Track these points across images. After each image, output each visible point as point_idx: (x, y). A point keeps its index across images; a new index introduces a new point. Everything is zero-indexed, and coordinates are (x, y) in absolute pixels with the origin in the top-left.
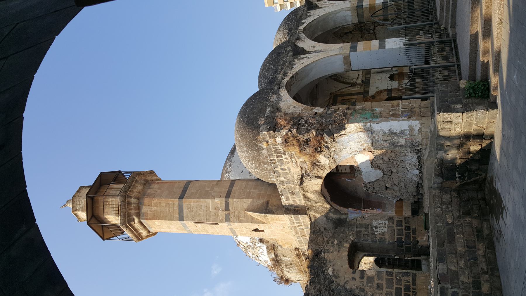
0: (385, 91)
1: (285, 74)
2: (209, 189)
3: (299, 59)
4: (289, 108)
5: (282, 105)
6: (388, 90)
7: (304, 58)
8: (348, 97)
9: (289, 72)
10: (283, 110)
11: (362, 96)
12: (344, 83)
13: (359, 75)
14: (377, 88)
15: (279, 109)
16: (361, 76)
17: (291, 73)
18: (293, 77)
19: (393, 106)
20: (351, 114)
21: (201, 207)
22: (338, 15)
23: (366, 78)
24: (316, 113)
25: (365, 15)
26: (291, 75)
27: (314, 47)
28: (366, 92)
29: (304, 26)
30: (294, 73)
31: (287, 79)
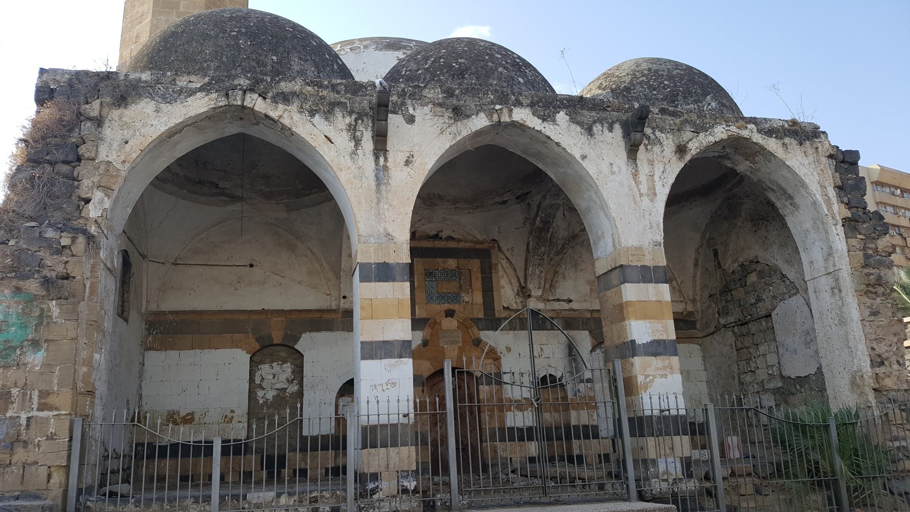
0: (499, 367)
1: (285, 98)
2: (181, 9)
3: (352, 129)
4: (124, 126)
6: (499, 375)
7: (357, 142)
8: (477, 284)
9: (294, 107)
10: (115, 113)
12: (526, 269)
13: (570, 301)
14: (509, 349)
16: (566, 306)
17: (291, 117)
18: (272, 119)
20: (18, 290)
21: (143, 4)
22: (602, 214)
24: (87, 201)
25: (608, 293)
26: (273, 114)
27: (407, 163)
28: (493, 323)
29: (534, 123)
30: (286, 121)
31: (260, 105)
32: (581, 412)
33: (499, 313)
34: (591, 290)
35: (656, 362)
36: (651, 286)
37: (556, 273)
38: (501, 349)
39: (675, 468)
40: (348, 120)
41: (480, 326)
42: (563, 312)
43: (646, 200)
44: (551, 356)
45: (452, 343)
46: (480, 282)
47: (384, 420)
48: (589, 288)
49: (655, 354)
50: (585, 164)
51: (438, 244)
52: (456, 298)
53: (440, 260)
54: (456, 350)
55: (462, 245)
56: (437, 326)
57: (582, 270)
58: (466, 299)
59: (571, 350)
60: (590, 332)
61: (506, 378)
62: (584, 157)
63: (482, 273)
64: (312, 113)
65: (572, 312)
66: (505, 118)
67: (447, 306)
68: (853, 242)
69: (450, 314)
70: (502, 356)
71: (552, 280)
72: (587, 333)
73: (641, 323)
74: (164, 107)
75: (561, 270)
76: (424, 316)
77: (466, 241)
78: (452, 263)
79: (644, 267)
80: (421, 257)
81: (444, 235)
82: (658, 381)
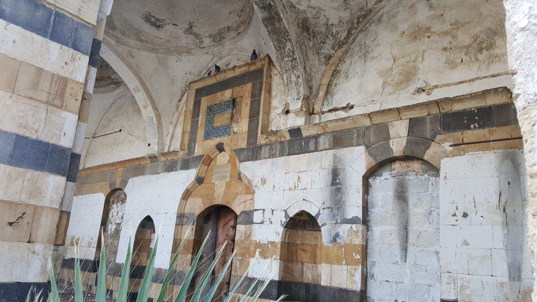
8: (245, 110)
11: (244, 145)
14: (264, 181)
23: (316, 137)
28: (253, 152)
32: (336, 267)
33: (261, 140)
34: (385, 83)
37: (335, 73)
38: (256, 181)
41: (242, 157)
42: (329, 125)
44: (309, 187)
45: (222, 178)
46: (249, 108)
48: (381, 81)
51: (221, 77)
52: (226, 130)
53: (219, 94)
54: (224, 186)
55: (238, 72)
56: (213, 163)
57: (373, 58)
58: (235, 130)
59: (336, 177)
60: (367, 147)
61: (257, 217)
63: (252, 97)
65: (341, 123)
67: (217, 140)
69: (220, 148)
70: (256, 189)
71: (329, 85)
75: (343, 67)
76: (200, 153)
77: (240, 67)
78: (228, 94)
80: (207, 95)
81: (231, 66)
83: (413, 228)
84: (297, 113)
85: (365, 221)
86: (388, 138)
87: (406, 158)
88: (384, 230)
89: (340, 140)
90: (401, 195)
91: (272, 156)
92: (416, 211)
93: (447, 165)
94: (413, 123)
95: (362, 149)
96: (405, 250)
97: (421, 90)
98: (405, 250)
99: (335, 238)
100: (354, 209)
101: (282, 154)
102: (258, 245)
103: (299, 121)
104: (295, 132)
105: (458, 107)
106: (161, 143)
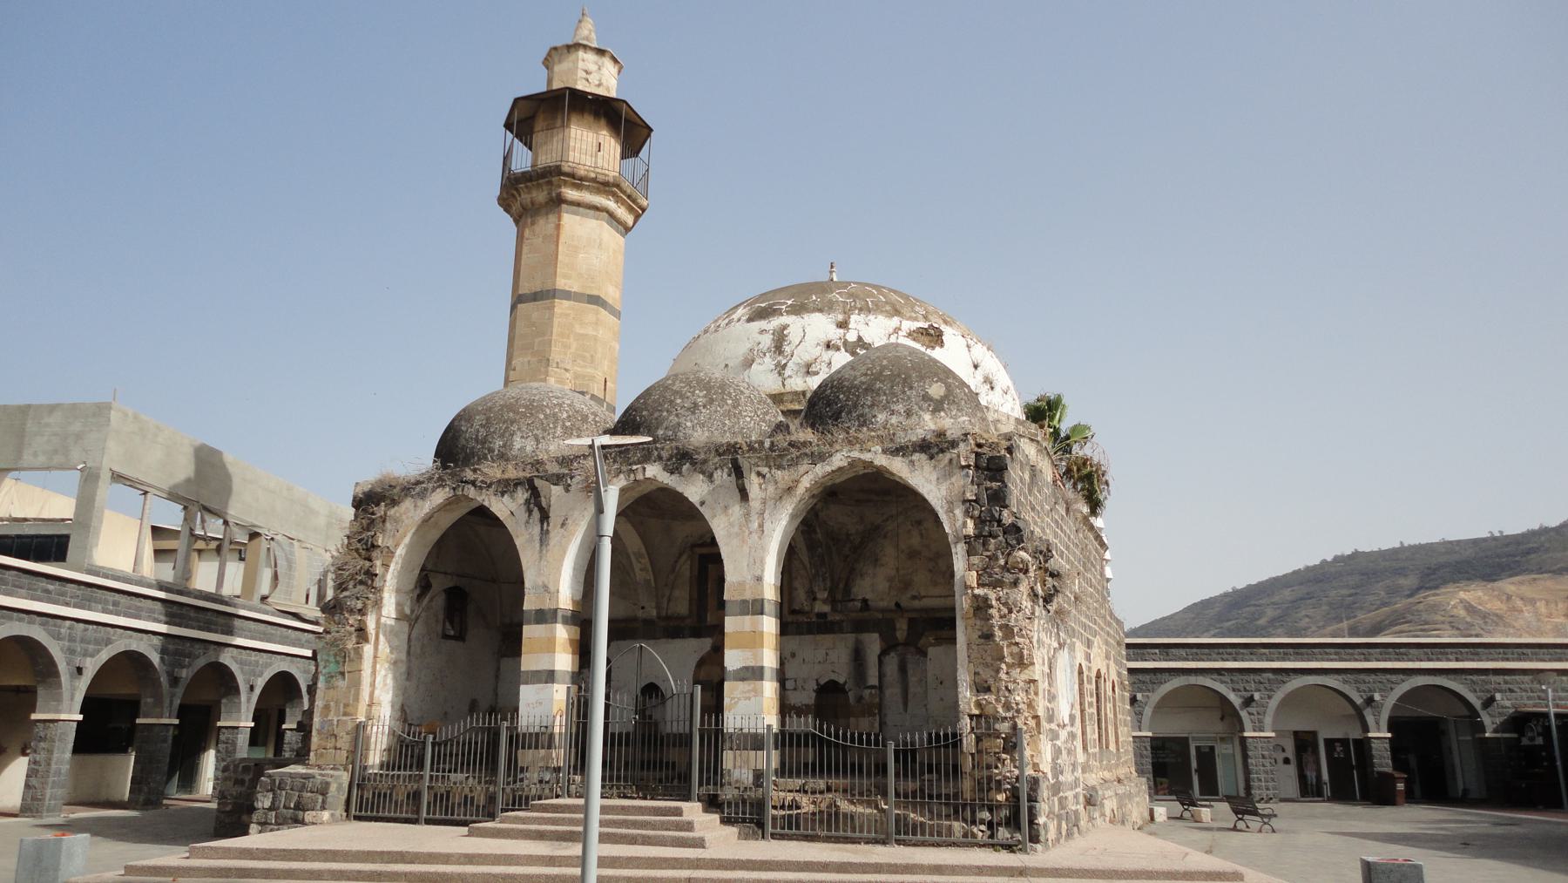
5: (407, 504)
10: (392, 512)
15: (394, 503)
19: (346, 705)
27: (563, 525)
35: (741, 686)
36: (748, 618)
39: (747, 777)
40: (526, 495)
43: (755, 536)
47: (531, 730)
49: (743, 679)
50: (702, 509)
59: (858, 656)
62: (702, 503)
64: (503, 494)
66: (640, 477)
68: (975, 560)
72: (876, 636)
73: (735, 652)
74: (420, 503)
79: (744, 602)
82: (742, 703)
83: (912, 690)
84: (825, 601)
85: (880, 687)
86: (894, 629)
87: (906, 644)
88: (893, 693)
89: (860, 627)
90: (903, 669)
91: (801, 633)
92: (913, 680)
93: (932, 651)
94: (911, 621)
95: (876, 636)
96: (905, 704)
97: (914, 597)
98: (905, 704)
99: (860, 699)
100: (873, 680)
101: (810, 632)
102: (793, 708)
103: (826, 608)
104: (822, 615)
105: (938, 615)
106: (658, 607)
